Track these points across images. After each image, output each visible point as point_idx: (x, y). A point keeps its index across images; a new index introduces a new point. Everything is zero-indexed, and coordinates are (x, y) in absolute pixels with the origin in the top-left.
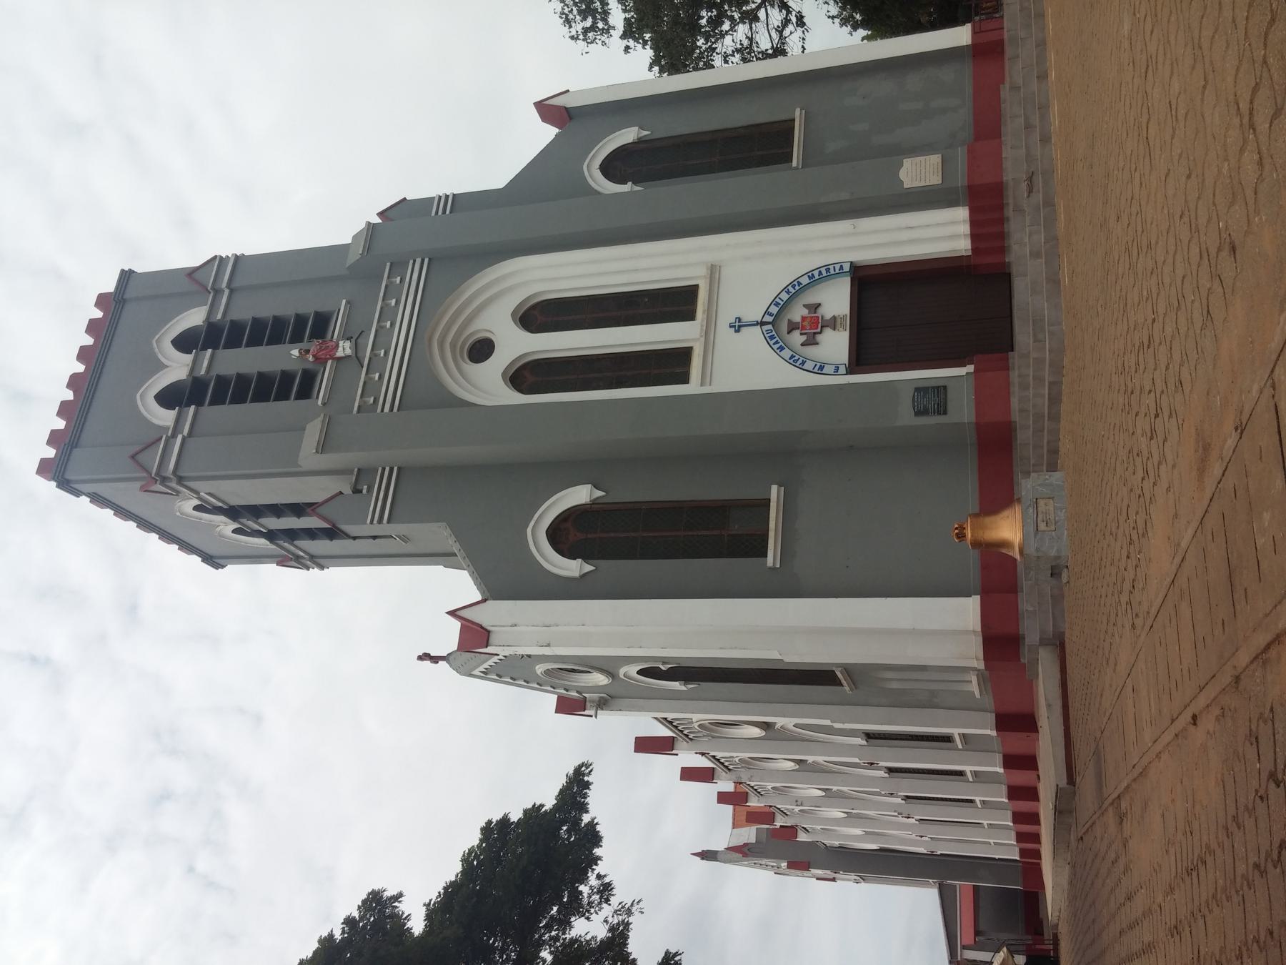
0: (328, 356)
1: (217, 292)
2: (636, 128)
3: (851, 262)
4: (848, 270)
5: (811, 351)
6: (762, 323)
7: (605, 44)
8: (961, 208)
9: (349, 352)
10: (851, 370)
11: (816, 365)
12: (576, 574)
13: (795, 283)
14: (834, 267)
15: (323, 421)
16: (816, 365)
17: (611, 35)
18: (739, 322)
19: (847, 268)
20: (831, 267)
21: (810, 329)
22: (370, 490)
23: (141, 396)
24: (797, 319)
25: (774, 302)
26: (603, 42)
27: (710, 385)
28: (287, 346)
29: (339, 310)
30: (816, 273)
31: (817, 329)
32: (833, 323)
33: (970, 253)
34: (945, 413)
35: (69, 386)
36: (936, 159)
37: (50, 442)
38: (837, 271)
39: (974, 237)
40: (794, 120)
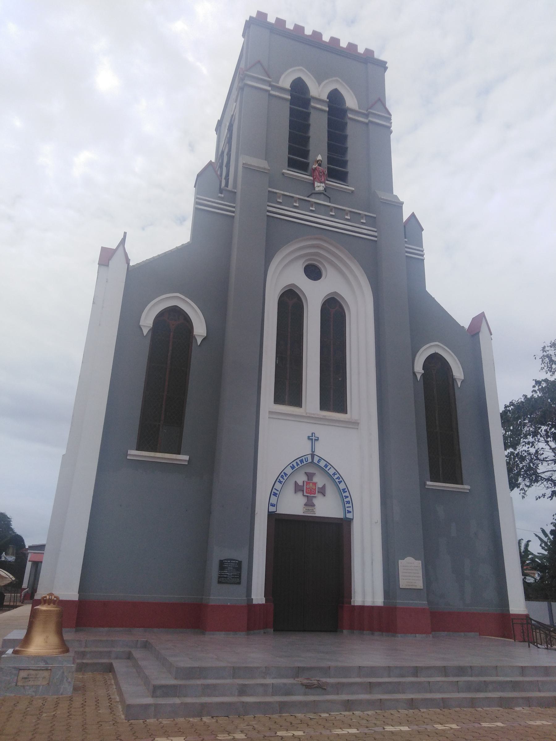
0: (315, 177)
1: (367, 116)
2: (463, 378)
5: (290, 487)
6: (313, 455)
7: (542, 370)
8: (383, 600)
9: (317, 189)
10: (271, 515)
11: (278, 491)
12: (142, 323)
13: (341, 479)
14: (350, 507)
15: (265, 169)
16: (278, 491)
17: (547, 373)
18: (315, 440)
19: (349, 516)
20: (350, 505)
21: (306, 487)
24: (315, 480)
25: (328, 464)
26: (544, 368)
27: (269, 418)
28: (326, 154)
29: (348, 186)
30: (347, 494)
32: (310, 504)
33: (352, 604)
34: (219, 582)
36: (419, 584)
37: (278, 20)
38: (347, 509)
39: (362, 608)
40: (462, 484)
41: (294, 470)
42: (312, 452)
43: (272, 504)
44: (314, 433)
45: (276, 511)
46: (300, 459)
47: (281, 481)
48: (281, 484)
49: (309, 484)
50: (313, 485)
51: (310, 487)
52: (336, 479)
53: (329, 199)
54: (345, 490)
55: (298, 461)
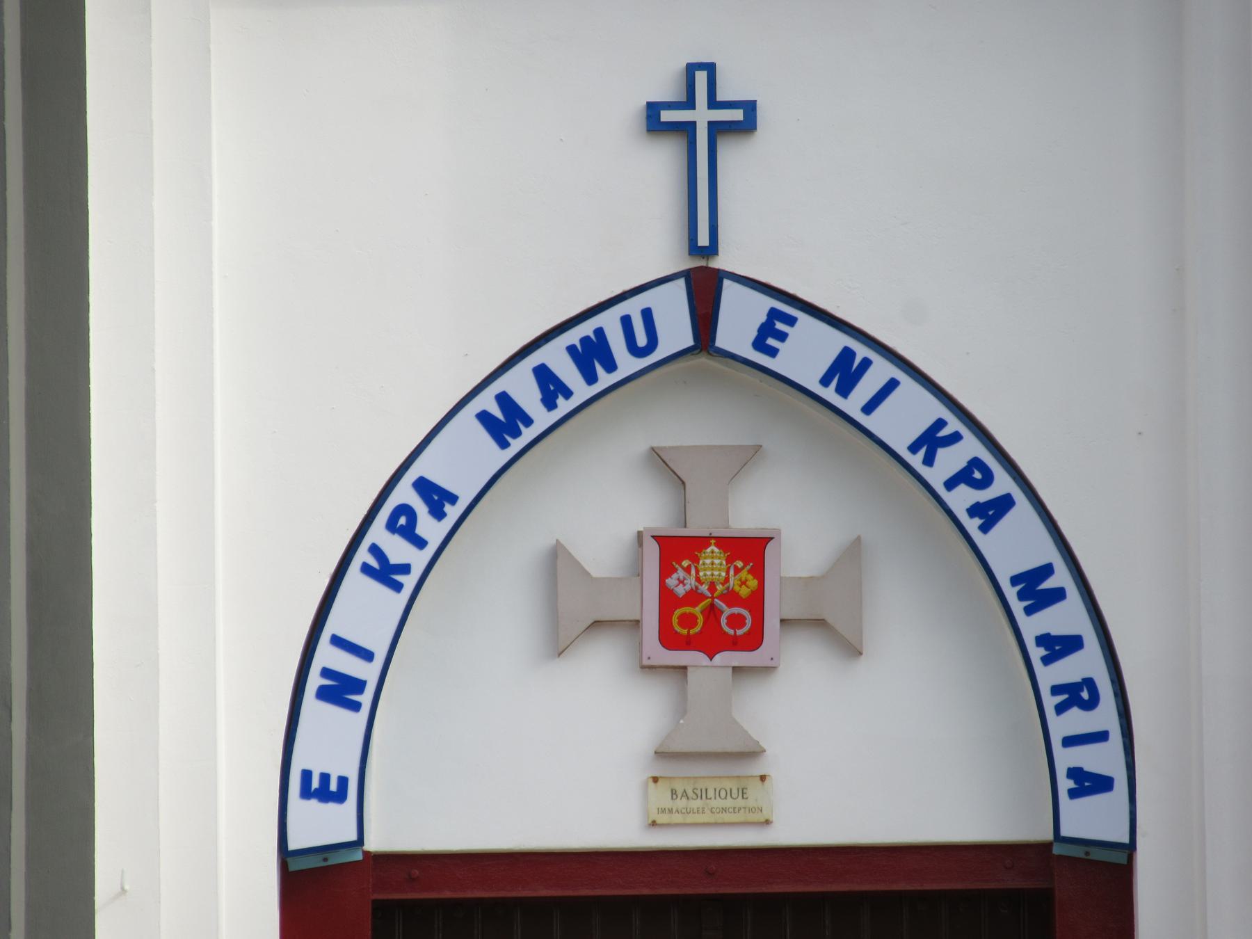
3: (1131, 847)
4: (1065, 832)
11: (367, 656)
14: (1102, 736)
16: (367, 656)
18: (716, 129)
20: (1105, 716)
25: (862, 351)
31: (669, 639)
41: (516, 445)
42: (694, 249)
43: (315, 784)
44: (710, 68)
45: (360, 841)
46: (573, 337)
47: (394, 559)
48: (398, 587)
49: (696, 560)
50: (730, 560)
51: (704, 589)
52: (951, 484)
54: (1048, 584)
55: (556, 357)
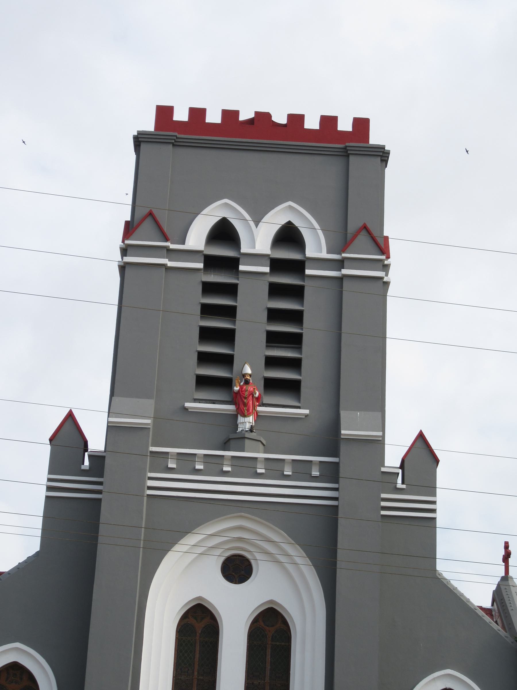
1: (340, 264)
22: (85, 473)
23: (226, 204)
35: (256, 113)
37: (193, 111)
53: (260, 443)
